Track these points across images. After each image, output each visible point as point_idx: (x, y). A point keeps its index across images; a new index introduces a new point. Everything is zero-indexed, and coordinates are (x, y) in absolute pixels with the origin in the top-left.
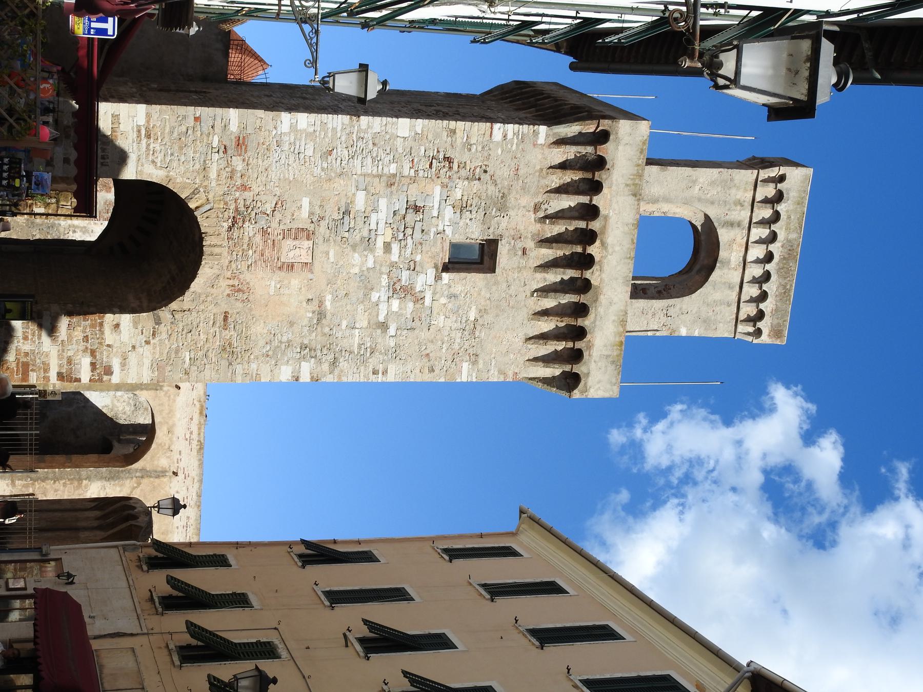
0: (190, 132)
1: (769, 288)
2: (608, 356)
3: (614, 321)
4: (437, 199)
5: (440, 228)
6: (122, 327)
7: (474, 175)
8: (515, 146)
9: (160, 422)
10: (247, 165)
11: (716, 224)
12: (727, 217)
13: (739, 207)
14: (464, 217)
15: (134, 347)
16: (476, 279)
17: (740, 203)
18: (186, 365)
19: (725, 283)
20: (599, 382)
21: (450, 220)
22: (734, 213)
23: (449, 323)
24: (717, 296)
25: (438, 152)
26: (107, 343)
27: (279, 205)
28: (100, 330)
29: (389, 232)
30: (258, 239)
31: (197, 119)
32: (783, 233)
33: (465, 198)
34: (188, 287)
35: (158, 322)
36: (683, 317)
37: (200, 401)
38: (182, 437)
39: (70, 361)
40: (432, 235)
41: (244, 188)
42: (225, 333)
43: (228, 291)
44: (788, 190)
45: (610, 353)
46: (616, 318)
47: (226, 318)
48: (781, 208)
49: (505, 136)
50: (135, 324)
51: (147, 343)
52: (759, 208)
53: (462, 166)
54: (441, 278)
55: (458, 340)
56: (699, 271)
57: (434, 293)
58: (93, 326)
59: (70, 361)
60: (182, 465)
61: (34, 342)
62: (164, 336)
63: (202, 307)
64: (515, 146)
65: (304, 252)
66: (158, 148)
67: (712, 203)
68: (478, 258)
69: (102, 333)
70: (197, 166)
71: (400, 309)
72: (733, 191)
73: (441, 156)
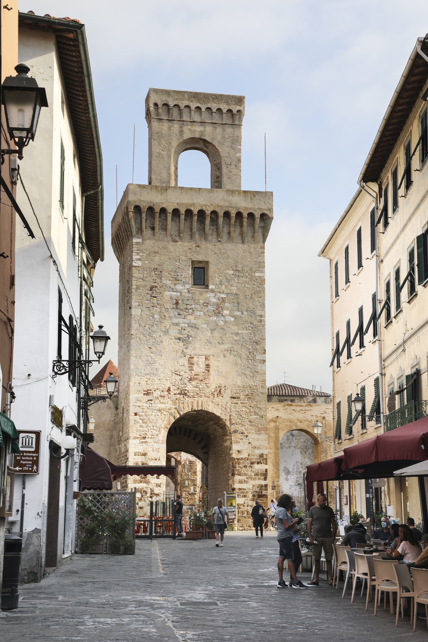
0: (142, 418)
1: (215, 107)
2: (251, 199)
3: (232, 197)
4: (172, 293)
5: (186, 291)
6: (239, 449)
7: (159, 275)
8: (143, 254)
9: (296, 426)
10: (157, 389)
11: (181, 140)
12: (177, 134)
13: (172, 128)
14: (180, 279)
15: (249, 443)
16: (212, 270)
17: (169, 128)
18: (258, 417)
19: (212, 133)
20: (265, 203)
21: (183, 286)
22: (175, 131)
23: (235, 284)
24: (219, 137)
25: (148, 294)
26: (247, 456)
27: (177, 373)
28: (241, 460)
29: (189, 317)
30: (194, 383)
31: (136, 414)
32: (185, 102)
33: (171, 279)
34: (219, 417)
35: (236, 431)
36: (231, 155)
37: (284, 406)
38: (304, 415)
39: (257, 475)
40: (190, 295)
41: (169, 390)
42: (241, 398)
43: (220, 397)
44: (162, 101)
45: (249, 198)
46: (231, 196)
47: (234, 398)
48: (171, 104)
49: (139, 260)
50: (238, 442)
51: (247, 436)
52: (172, 116)
53: (155, 281)
54: (212, 289)
55: (244, 279)
56: (207, 147)
57: (220, 292)
58: (239, 463)
59: (257, 475)
60: (319, 415)
61: (247, 492)
62: (243, 428)
63: (229, 410)
64: (143, 254)
65: (200, 360)
66: (150, 433)
67: (170, 143)
68: (200, 274)
69: (242, 459)
70: (159, 414)
71: (228, 310)
72: (164, 132)
73: (150, 292)
